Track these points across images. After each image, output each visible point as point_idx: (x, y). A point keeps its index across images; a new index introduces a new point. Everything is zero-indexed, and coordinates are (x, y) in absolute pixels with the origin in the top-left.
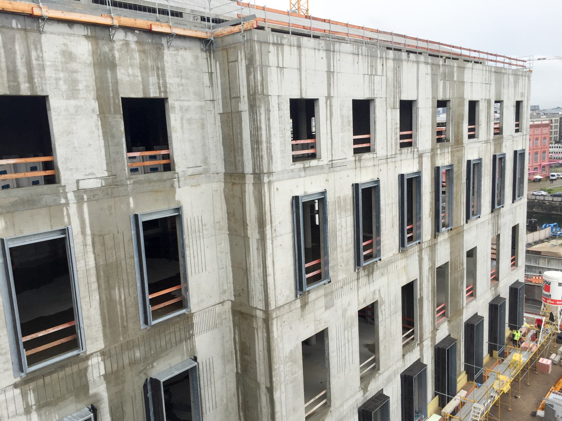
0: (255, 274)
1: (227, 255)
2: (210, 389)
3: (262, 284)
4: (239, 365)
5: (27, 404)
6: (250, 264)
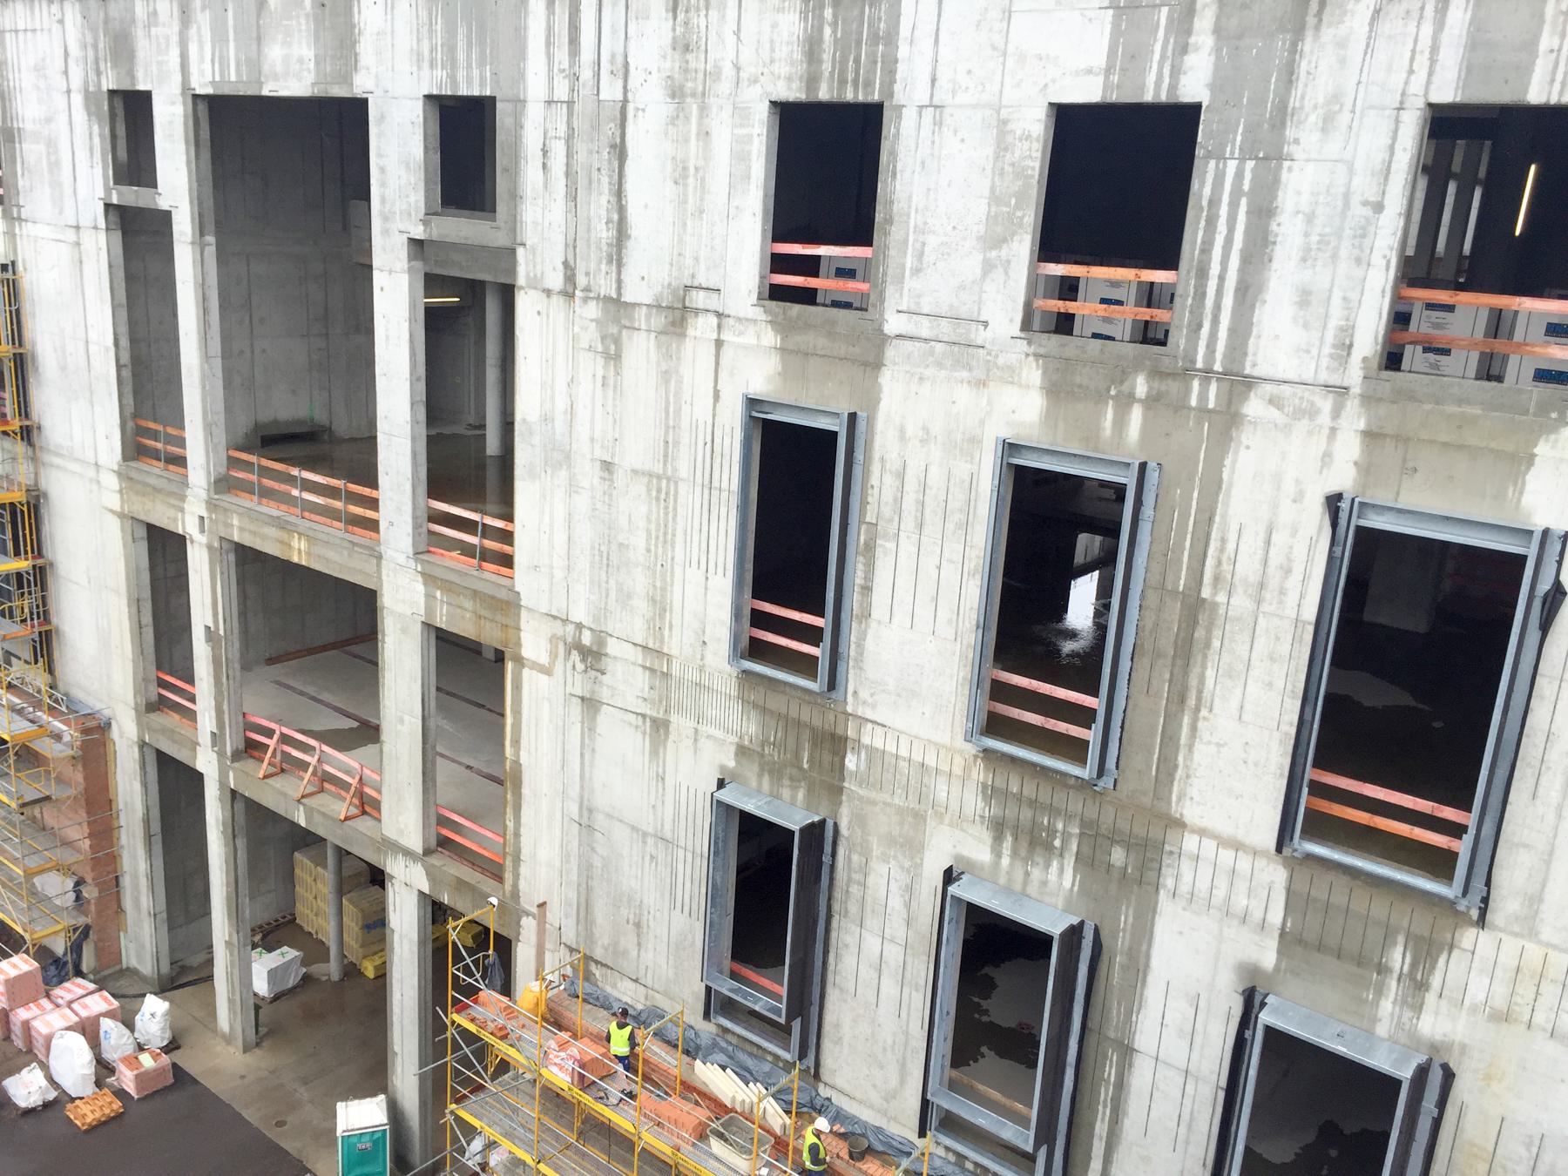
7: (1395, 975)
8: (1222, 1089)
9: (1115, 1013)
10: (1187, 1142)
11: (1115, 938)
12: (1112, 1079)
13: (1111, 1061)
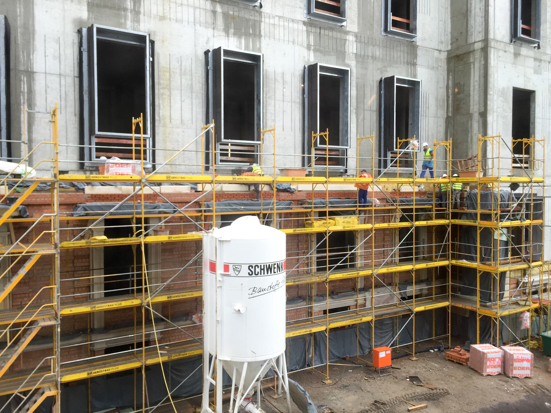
0: (476, 11)
1: (446, 10)
2: (424, 121)
3: (483, 15)
4: (450, 109)
5: (309, 42)
6: (471, 4)
7: (129, 11)
8: (76, 77)
9: (22, 57)
10: (66, 107)
11: (16, 20)
12: (26, 90)
13: (24, 81)
